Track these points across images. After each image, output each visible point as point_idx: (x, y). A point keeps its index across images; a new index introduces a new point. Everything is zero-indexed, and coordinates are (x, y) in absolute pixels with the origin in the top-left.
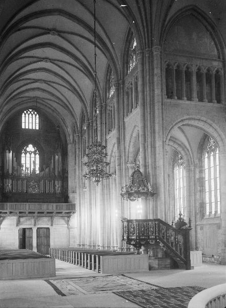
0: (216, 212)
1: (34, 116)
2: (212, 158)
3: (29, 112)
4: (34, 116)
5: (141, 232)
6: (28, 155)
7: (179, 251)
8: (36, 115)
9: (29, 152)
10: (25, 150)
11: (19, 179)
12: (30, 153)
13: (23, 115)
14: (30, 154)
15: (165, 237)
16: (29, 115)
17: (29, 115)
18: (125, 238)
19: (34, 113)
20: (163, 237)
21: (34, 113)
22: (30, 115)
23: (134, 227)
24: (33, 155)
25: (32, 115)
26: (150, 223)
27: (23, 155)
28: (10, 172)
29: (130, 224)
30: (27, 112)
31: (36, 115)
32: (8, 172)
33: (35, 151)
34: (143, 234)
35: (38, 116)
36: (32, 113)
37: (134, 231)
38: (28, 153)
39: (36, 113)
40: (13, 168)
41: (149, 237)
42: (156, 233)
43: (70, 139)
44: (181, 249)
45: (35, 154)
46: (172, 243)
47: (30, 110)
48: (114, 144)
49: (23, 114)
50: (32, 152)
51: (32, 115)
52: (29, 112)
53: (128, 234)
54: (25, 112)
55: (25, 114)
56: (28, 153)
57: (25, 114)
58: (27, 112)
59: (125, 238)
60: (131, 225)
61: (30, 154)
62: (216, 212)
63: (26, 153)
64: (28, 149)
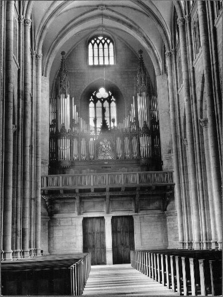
1: (106, 45)
3: (98, 41)
4: (106, 45)
6: (99, 104)
8: (108, 45)
9: (100, 99)
10: (95, 97)
11: (82, 137)
12: (103, 100)
13: (90, 46)
14: (102, 102)
16: (98, 45)
17: (98, 45)
19: (106, 41)
21: (106, 41)
22: (101, 45)
24: (106, 104)
25: (103, 45)
27: (92, 105)
28: (68, 127)
30: (95, 41)
31: (108, 45)
32: (63, 127)
33: (110, 97)
35: (111, 45)
36: (103, 41)
38: (99, 101)
39: (108, 41)
40: (72, 120)
43: (157, 67)
45: (110, 102)
47: (101, 38)
49: (90, 45)
50: (105, 100)
51: (103, 45)
52: (98, 41)
54: (93, 41)
55: (93, 45)
56: (99, 101)
57: (93, 45)
58: (95, 41)
61: (102, 102)
63: (96, 100)
64: (99, 95)
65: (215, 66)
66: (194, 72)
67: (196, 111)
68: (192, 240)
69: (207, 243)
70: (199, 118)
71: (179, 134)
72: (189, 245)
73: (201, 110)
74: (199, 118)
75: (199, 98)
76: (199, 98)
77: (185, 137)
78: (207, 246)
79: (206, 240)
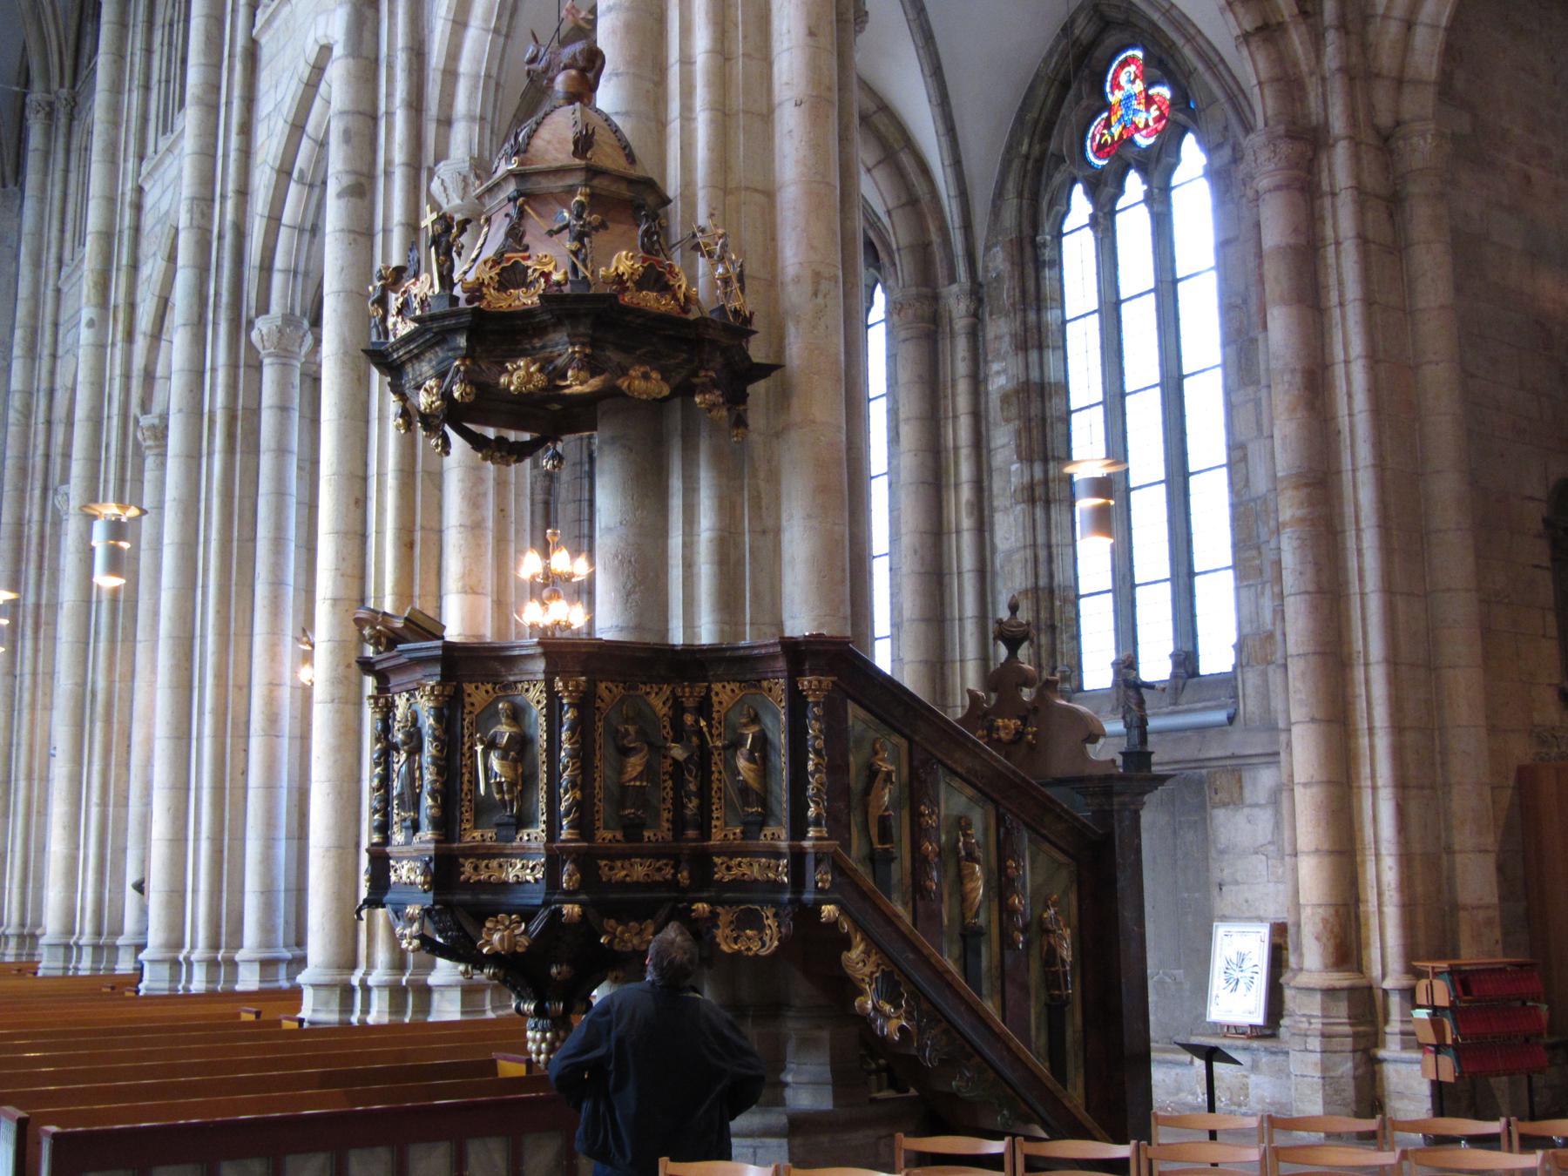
0: (1186, 660)
2: (1133, 223)
5: (623, 795)
7: (1040, 1039)
15: (900, 870)
18: (406, 872)
20: (879, 861)
23: (520, 747)
26: (724, 694)
29: (477, 695)
34: (632, 830)
37: (523, 782)
41: (702, 862)
42: (798, 828)
44: (1055, 1012)
46: (970, 938)
48: (318, 69)
53: (445, 825)
59: (406, 872)
60: (489, 715)
62: (1186, 660)
65: (230, 205)
66: (138, 207)
67: (127, 376)
68: (38, 923)
69: (97, 948)
70: (135, 409)
71: (39, 461)
72: (21, 945)
73: (149, 376)
74: (135, 409)
75: (144, 321)
76: (144, 321)
77: (65, 479)
78: (96, 959)
79: (98, 932)
